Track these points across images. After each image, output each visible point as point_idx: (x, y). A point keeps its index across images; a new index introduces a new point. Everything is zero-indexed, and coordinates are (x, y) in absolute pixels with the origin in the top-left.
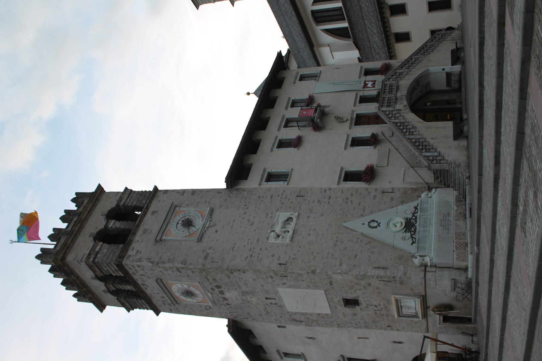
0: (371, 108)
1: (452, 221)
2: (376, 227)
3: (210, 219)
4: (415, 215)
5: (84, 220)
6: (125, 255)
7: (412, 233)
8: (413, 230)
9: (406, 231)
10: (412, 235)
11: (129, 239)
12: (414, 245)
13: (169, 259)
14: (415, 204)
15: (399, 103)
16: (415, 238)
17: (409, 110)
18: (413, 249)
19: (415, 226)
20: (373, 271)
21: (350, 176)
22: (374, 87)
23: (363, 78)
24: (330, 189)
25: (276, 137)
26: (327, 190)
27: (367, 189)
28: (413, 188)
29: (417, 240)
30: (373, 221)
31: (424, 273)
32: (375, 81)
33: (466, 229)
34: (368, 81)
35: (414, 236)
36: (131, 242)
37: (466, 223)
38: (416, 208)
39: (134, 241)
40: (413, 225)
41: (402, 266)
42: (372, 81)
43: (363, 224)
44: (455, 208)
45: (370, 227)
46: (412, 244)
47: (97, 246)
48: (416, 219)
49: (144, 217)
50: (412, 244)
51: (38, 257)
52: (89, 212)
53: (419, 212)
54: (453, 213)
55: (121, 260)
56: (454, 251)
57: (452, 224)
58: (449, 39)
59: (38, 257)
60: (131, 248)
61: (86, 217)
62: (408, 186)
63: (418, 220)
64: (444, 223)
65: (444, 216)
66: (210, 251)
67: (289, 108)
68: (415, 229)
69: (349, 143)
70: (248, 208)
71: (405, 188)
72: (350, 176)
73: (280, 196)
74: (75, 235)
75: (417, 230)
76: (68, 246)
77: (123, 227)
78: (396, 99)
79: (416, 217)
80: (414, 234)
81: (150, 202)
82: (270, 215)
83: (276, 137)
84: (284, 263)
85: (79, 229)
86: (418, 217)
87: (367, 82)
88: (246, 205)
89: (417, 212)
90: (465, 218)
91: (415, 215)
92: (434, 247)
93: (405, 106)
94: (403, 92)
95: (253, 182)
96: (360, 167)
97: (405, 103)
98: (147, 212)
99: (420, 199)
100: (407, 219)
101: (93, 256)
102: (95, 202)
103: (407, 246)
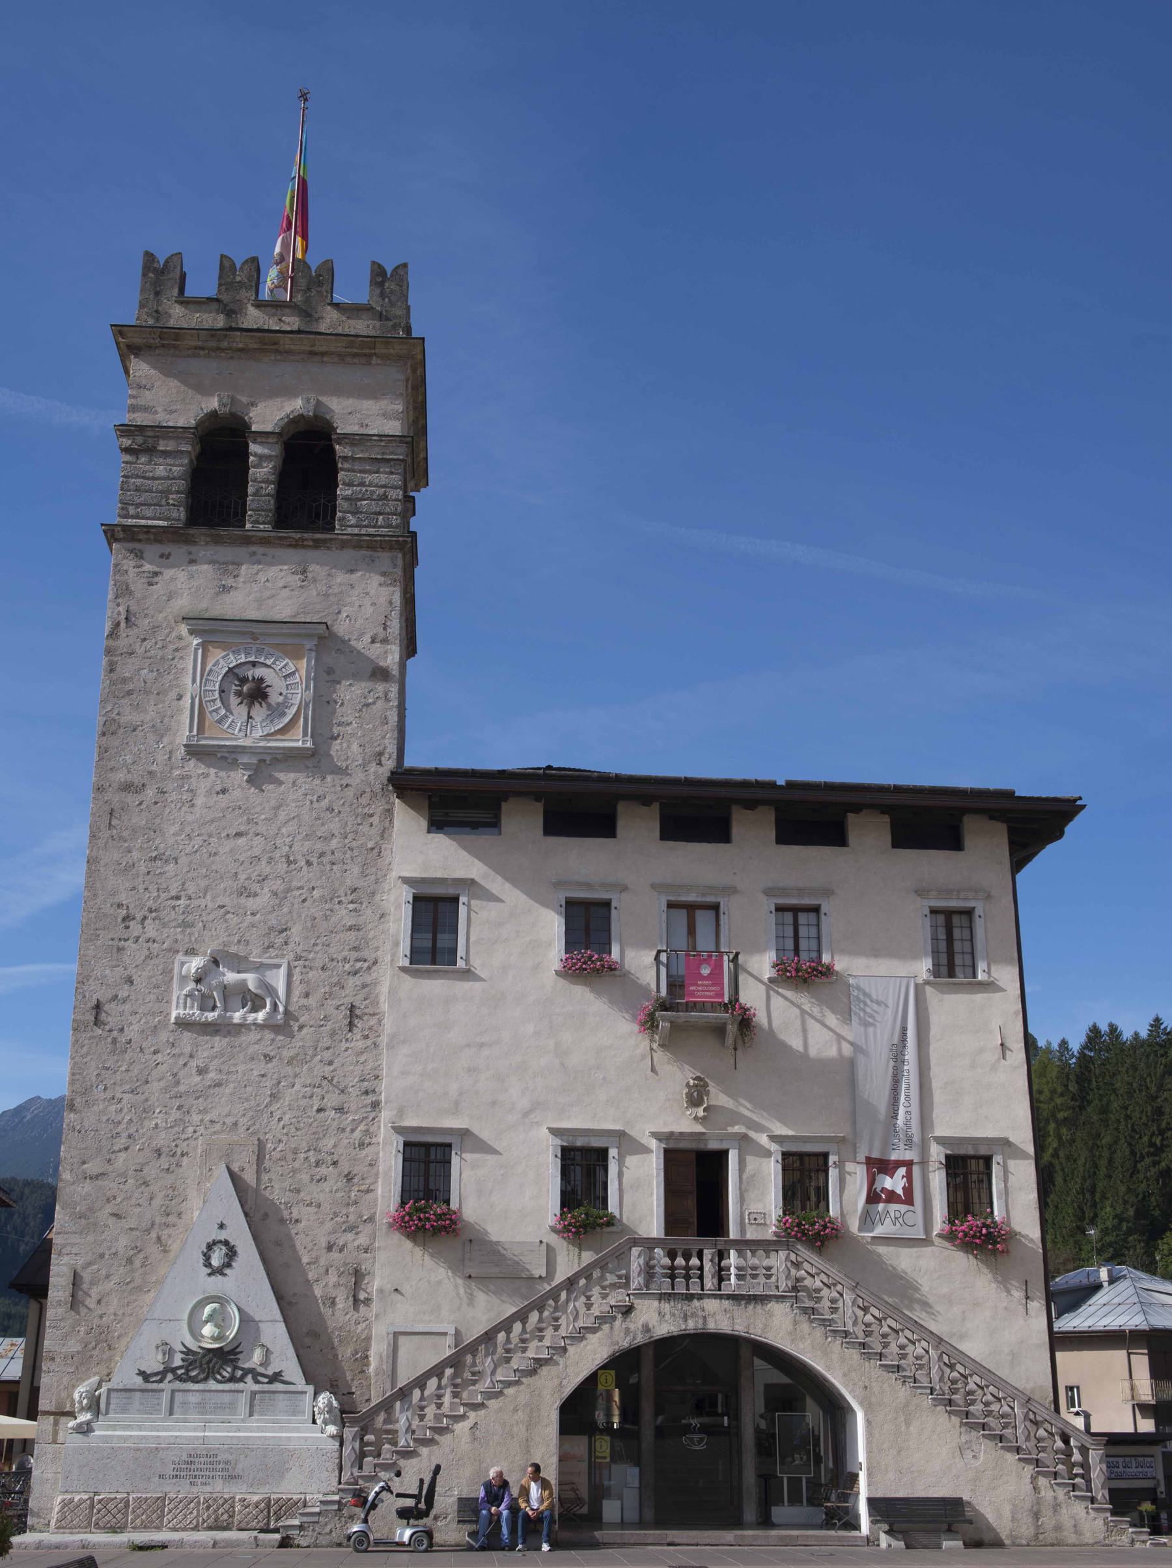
0: (756, 1195)
1: (208, 1489)
2: (208, 1264)
3: (268, 758)
4: (249, 1378)
5: (278, 352)
6: (140, 541)
7: (180, 1372)
8: (193, 1373)
9: (189, 1352)
10: (174, 1370)
11: (192, 531)
12: (139, 1380)
13: (124, 680)
14: (292, 1370)
15: (666, 1307)
16: (161, 1381)
17: (625, 1343)
18: (125, 1375)
19: (206, 1379)
20: (65, 1269)
21: (428, 1162)
22: (873, 1198)
23: (937, 1153)
24: (375, 1105)
25: (624, 888)
26: (371, 1098)
27: (371, 1219)
28: (368, 1365)
29: (155, 1386)
30: (232, 1253)
31: (53, 1409)
32: (908, 1199)
33: (175, 1529)
34: (909, 1176)
35: (170, 1376)
36: (189, 541)
37: (196, 1528)
38: (276, 1377)
39: (193, 549)
40: (209, 1373)
41: (79, 1347)
42: (908, 1190)
43: (222, 1226)
44: (256, 1498)
45: (210, 1247)
46: (142, 1373)
47: (177, 438)
48: (232, 1379)
49: (282, 546)
50: (142, 1373)
51: (149, 257)
52: (312, 353)
53: (257, 1387)
54: (238, 1491)
55: (121, 535)
56: (96, 1493)
57: (195, 1489)
58: (1047, 1494)
59: (149, 257)
60: (167, 549)
61: (288, 352)
62: (377, 1351)
63: (227, 1386)
64: (196, 1464)
65: (226, 1463)
66: (150, 793)
67: (770, 904)
68: (195, 1380)
69: (579, 1143)
70: (309, 863)
71: (368, 1339)
72: (428, 1162)
73: (354, 955)
74: (219, 349)
75: (190, 1386)
76: (174, 347)
77: (251, 490)
78: (689, 1297)
79: (241, 1379)
80: (180, 1379)
81: (343, 545)
82: (279, 940)
83: (624, 888)
84: (103, 1016)
85: (241, 350)
86: (241, 1386)
87: (902, 1171)
88: (322, 855)
89: (257, 1382)
90: (210, 1528)
91: (249, 1378)
92: (119, 1437)
93: (647, 1329)
94: (719, 1317)
95: (421, 851)
96: (470, 1187)
97: (663, 1329)
98: (304, 547)
99: (310, 1389)
100: (234, 1352)
101: (140, 440)
102: (355, 355)
103: (141, 1353)
